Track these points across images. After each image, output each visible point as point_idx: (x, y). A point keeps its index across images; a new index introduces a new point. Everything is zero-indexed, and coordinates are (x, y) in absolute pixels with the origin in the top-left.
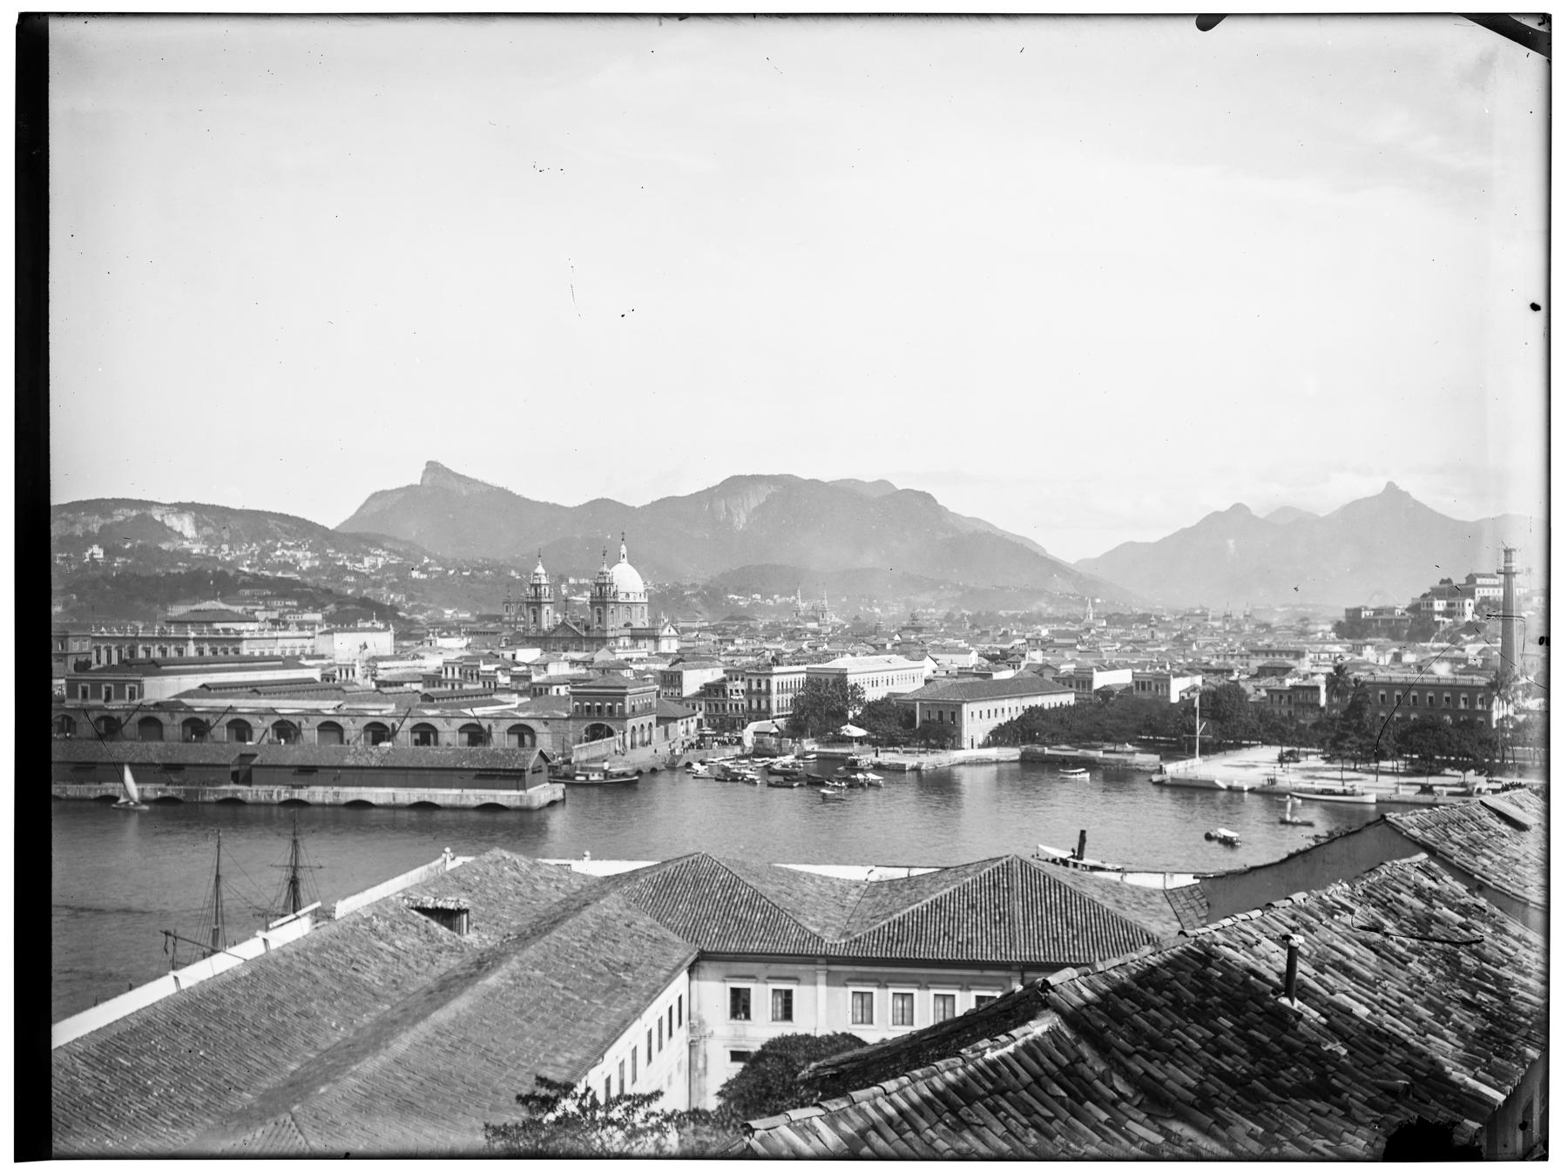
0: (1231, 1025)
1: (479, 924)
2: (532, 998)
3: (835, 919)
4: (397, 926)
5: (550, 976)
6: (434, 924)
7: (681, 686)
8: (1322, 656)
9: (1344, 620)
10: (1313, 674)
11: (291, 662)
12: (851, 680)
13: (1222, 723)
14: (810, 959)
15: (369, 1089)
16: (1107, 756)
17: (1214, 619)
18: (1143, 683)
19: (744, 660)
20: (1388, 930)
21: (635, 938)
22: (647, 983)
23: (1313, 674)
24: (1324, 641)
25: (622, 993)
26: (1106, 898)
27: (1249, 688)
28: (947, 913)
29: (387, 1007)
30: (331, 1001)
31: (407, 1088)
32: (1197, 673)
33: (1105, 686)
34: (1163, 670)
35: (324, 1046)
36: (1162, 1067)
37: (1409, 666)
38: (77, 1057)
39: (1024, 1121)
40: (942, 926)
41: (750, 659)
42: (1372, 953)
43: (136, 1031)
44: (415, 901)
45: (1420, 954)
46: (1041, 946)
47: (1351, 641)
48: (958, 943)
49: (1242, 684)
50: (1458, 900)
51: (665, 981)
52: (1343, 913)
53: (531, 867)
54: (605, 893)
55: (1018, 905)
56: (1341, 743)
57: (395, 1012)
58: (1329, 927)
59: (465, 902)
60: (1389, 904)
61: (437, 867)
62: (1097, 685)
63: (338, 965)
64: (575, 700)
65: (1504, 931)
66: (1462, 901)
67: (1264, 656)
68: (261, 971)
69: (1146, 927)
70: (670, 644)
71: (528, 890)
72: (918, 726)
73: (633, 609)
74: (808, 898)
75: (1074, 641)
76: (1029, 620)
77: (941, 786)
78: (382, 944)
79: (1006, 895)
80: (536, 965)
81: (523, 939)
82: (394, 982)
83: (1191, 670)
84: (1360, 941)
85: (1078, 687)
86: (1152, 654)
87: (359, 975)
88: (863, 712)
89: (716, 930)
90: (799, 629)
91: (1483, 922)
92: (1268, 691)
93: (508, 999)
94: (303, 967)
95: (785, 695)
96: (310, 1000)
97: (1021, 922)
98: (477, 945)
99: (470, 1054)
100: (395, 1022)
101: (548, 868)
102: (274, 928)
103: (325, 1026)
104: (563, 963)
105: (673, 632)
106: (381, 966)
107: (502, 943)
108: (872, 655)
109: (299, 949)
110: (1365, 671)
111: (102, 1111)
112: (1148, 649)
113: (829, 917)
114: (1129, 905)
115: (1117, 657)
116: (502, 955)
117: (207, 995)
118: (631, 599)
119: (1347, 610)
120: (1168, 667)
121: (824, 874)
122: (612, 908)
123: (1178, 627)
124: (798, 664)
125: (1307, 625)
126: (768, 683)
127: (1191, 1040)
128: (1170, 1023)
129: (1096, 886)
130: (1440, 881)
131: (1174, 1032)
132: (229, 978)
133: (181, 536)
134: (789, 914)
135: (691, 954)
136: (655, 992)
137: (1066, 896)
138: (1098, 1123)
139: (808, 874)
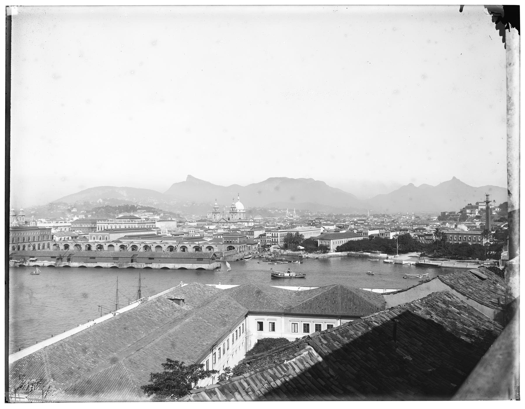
2: (198, 325)
5: (204, 319)
6: (174, 303)
8: (434, 226)
10: (431, 231)
16: (372, 254)
17: (403, 216)
18: (382, 234)
19: (271, 228)
21: (230, 307)
24: (435, 221)
26: (365, 296)
27: (412, 235)
29: (158, 327)
32: (398, 231)
38: (67, 343)
43: (85, 335)
44: (169, 297)
49: (411, 234)
52: (417, 310)
53: (204, 287)
55: (339, 298)
61: (179, 287)
64: (224, 239)
65: (473, 315)
67: (417, 225)
71: (202, 293)
75: (363, 222)
76: (352, 216)
78: (159, 309)
80: (200, 316)
81: (199, 307)
83: (396, 230)
86: (385, 226)
87: (151, 318)
91: (465, 311)
93: (191, 326)
94: (135, 316)
96: (136, 326)
98: (186, 309)
99: (178, 342)
104: (208, 315)
105: (252, 220)
107: (193, 309)
110: (446, 230)
113: (286, 302)
116: (192, 312)
117: (106, 324)
119: (441, 213)
123: (393, 218)
125: (430, 217)
130: (452, 298)
134: (274, 301)
135: (246, 312)
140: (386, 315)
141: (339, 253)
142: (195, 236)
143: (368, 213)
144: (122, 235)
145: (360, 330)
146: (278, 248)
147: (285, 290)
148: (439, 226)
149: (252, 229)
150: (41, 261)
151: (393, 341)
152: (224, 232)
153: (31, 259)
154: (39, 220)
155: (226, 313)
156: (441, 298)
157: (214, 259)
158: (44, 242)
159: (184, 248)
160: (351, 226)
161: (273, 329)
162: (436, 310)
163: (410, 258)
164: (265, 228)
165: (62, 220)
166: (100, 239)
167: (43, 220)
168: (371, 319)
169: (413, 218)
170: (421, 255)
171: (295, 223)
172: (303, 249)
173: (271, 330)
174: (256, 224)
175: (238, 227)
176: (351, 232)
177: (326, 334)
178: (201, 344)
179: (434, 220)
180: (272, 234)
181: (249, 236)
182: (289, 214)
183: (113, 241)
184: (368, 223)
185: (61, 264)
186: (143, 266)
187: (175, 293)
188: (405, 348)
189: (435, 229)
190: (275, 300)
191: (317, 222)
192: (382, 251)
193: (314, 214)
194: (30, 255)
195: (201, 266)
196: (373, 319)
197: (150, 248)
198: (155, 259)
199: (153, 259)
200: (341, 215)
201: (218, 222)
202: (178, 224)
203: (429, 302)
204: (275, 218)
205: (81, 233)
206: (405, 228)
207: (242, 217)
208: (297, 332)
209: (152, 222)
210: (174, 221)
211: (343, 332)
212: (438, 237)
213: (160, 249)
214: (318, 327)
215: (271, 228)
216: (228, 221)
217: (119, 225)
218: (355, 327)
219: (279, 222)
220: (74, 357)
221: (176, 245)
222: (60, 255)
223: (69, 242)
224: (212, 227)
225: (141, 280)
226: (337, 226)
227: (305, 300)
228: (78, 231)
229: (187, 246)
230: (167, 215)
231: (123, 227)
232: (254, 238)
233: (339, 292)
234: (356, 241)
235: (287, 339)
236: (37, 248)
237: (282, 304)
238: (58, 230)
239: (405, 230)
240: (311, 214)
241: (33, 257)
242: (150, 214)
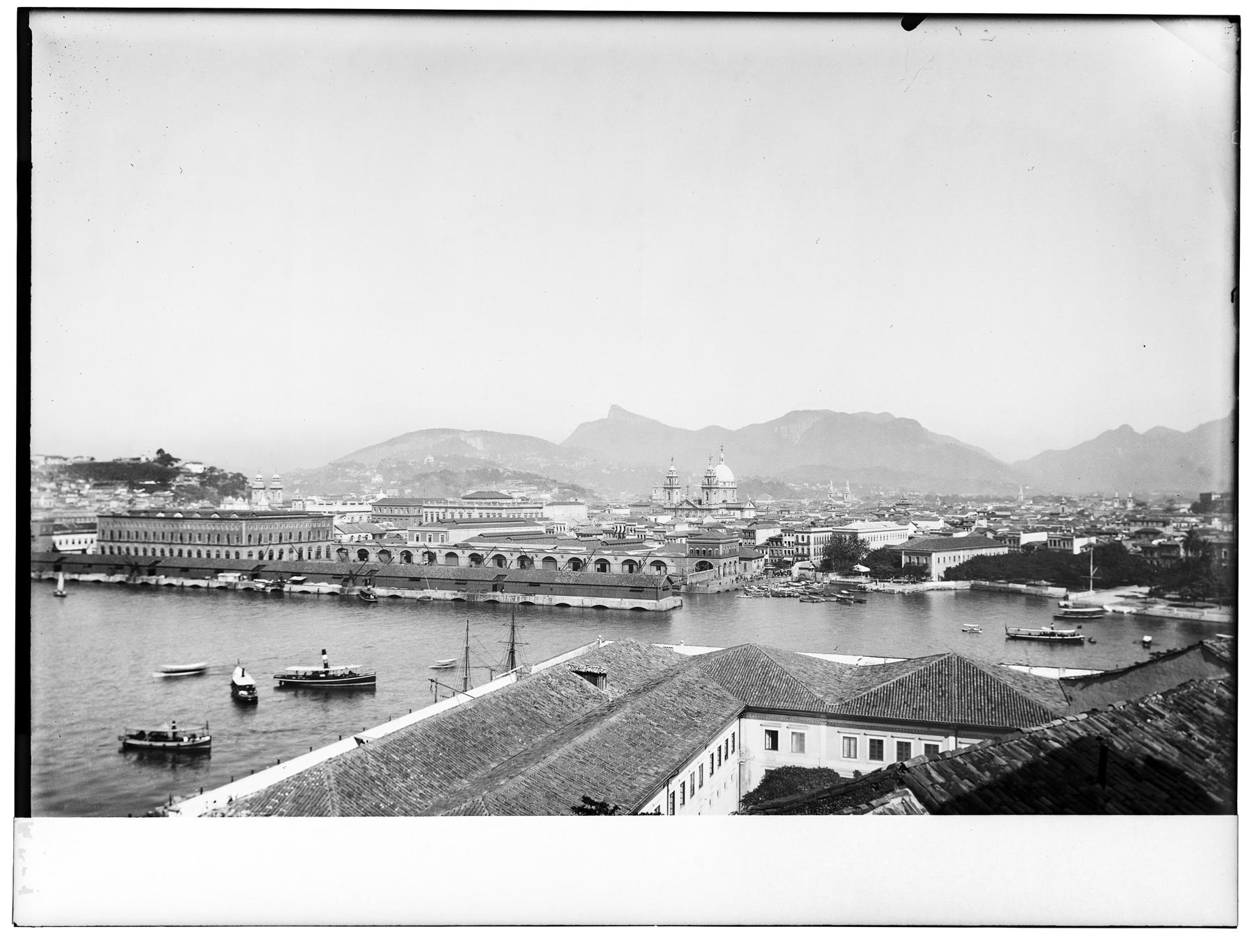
0: (1050, 803)
3: (834, 689)
6: (585, 682)
7: (755, 539)
8: (1183, 525)
9: (1199, 501)
10: (1175, 537)
11: (526, 522)
12: (861, 537)
15: (531, 784)
16: (1030, 588)
17: (1107, 500)
19: (795, 523)
20: (1191, 732)
21: (706, 696)
22: (710, 725)
23: (1175, 537)
26: (1016, 684)
27: (1129, 545)
28: (907, 689)
30: (518, 725)
31: (554, 784)
32: (1092, 536)
33: (1028, 543)
34: (1069, 533)
35: (513, 754)
40: (903, 697)
41: (799, 523)
42: (1176, 750)
43: (405, 739)
45: (1217, 751)
46: (970, 714)
47: (1204, 515)
48: (913, 709)
49: (1124, 543)
51: (721, 724)
52: (1155, 718)
56: (1194, 583)
57: (557, 735)
58: (1142, 728)
59: (604, 669)
60: (1195, 712)
61: (594, 646)
63: (526, 704)
67: (1140, 523)
68: (481, 705)
69: (1043, 705)
70: (750, 513)
72: (903, 566)
74: (817, 675)
75: (1009, 513)
76: (981, 500)
77: (918, 601)
78: (553, 693)
79: (947, 679)
80: (641, 710)
81: (637, 693)
82: (559, 716)
83: (1088, 533)
84: (1167, 740)
85: (1010, 542)
86: (1061, 523)
87: (538, 711)
88: (869, 556)
89: (757, 693)
90: (831, 505)
92: (1142, 548)
93: (622, 731)
94: (505, 705)
95: (819, 545)
96: (508, 725)
97: (956, 697)
100: (555, 741)
105: (752, 506)
106: (552, 706)
107: (625, 696)
108: (875, 521)
110: (1213, 535)
111: (380, 786)
112: (1060, 519)
113: (830, 688)
115: (1038, 524)
116: (623, 703)
117: (447, 720)
118: (727, 486)
120: (1073, 531)
121: (829, 660)
123: (1081, 505)
124: (827, 526)
125: (1172, 504)
126: (808, 537)
129: (1009, 675)
131: (1002, 807)
132: (460, 709)
134: (804, 685)
136: (715, 733)
137: (987, 681)
140: (1081, 726)
141: (952, 584)
143: (1021, 492)
144: (475, 533)
145: (1020, 757)
146: (810, 569)
147: (829, 663)
149: (751, 525)
150: (312, 584)
151: (1098, 786)
153: (295, 578)
154: (309, 498)
156: (1212, 692)
157: (668, 589)
158: (320, 544)
159: (603, 565)
160: (981, 522)
161: (802, 749)
162: (1201, 719)
163: (1122, 599)
164: (781, 522)
165: (353, 499)
166: (430, 540)
167: (317, 499)
168: (1045, 733)
169: (1130, 506)
170: (1151, 594)
171: (848, 514)
172: (866, 572)
173: (794, 750)
174: (759, 513)
175: (720, 521)
176: (978, 535)
177: (942, 762)
178: (643, 771)
179: (1182, 511)
181: (745, 541)
182: (836, 494)
183: (456, 546)
185: (353, 591)
186: (516, 600)
187: (587, 660)
188: (1128, 803)
189: (1184, 534)
191: (899, 513)
192: (1050, 581)
193: (893, 494)
194: (293, 570)
195: (640, 603)
196: (1048, 732)
197: (532, 561)
198: (541, 585)
199: (537, 584)
200: (956, 499)
201: (675, 509)
202: (591, 511)
203: (1184, 701)
204: (803, 501)
205: (391, 526)
206: (1113, 529)
207: (731, 498)
208: (856, 757)
210: (582, 504)
211: (979, 758)
212: (1191, 552)
213: (551, 565)
214: (904, 749)
215: (795, 523)
216: (698, 506)
217: (467, 511)
218: (1009, 749)
219: (812, 511)
221: (585, 557)
222: (351, 571)
223: (367, 544)
224: (663, 519)
225: (516, 629)
226: (947, 522)
227: (874, 686)
228: (385, 523)
229: (610, 559)
231: (475, 514)
232: (757, 545)
233: (955, 671)
234: (991, 557)
235: (835, 771)
236: (305, 556)
238: (347, 520)
239: (1110, 534)
240: (885, 494)
241: (299, 574)
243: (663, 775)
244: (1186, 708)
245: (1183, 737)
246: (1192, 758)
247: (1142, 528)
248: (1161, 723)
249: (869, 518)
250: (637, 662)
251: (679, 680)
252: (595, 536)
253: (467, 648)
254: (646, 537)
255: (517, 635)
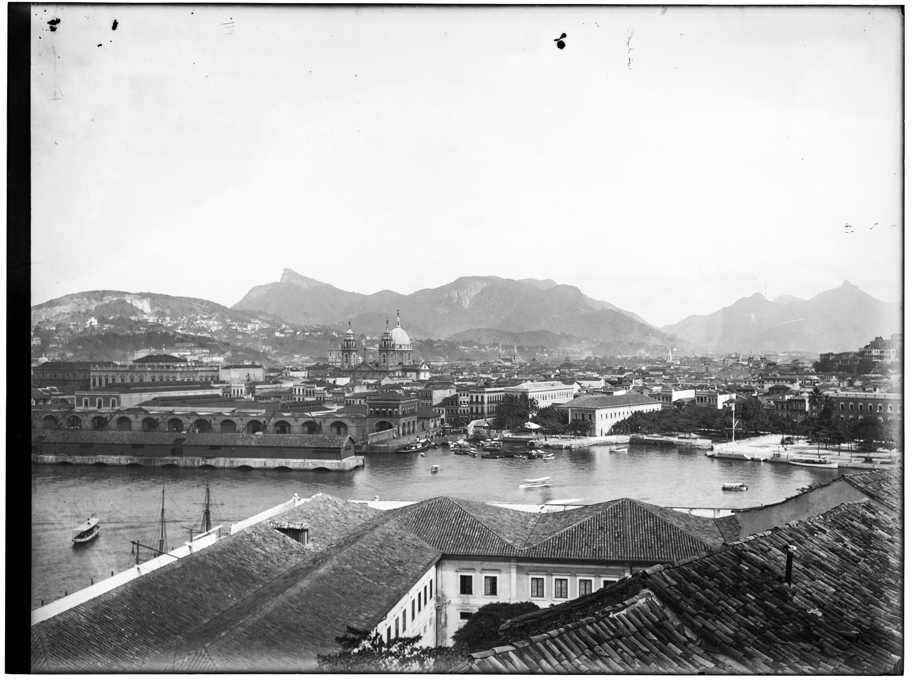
0: (754, 598)
1: (314, 538)
3: (522, 535)
4: (267, 539)
5: (355, 568)
6: (289, 538)
8: (807, 382)
10: (802, 393)
12: (530, 396)
13: (748, 421)
14: (507, 559)
16: (681, 440)
18: (702, 398)
19: (469, 383)
21: (405, 546)
23: (802, 393)
25: (397, 578)
26: (680, 524)
27: (764, 401)
28: (587, 532)
29: (261, 586)
30: (228, 583)
31: (272, 633)
32: (733, 392)
33: (679, 400)
34: (713, 391)
35: (224, 609)
36: (713, 623)
37: (858, 388)
38: (82, 615)
39: (633, 654)
40: (584, 539)
41: (472, 383)
42: (836, 556)
44: (277, 524)
45: (865, 557)
48: (593, 549)
49: (759, 398)
50: (887, 525)
51: (422, 571)
52: (820, 533)
54: (387, 520)
57: (265, 589)
59: (306, 525)
62: (674, 399)
63: (232, 561)
64: (370, 408)
66: (890, 526)
67: (773, 382)
69: (704, 541)
70: (425, 374)
72: (570, 423)
73: (404, 355)
74: (506, 523)
78: (258, 549)
79: (622, 521)
80: (347, 562)
82: (265, 571)
83: (730, 390)
84: (830, 549)
85: (663, 400)
87: (245, 568)
89: (452, 542)
90: (500, 366)
94: (212, 562)
96: (216, 582)
97: (630, 537)
98: (313, 550)
100: (265, 595)
101: (354, 505)
102: (195, 540)
103: (224, 597)
104: (363, 561)
105: (427, 368)
107: (327, 549)
108: (543, 381)
109: (209, 553)
110: (832, 390)
111: (96, 646)
112: (704, 378)
113: (518, 535)
114: (694, 528)
115: (686, 382)
118: (403, 348)
120: (716, 389)
121: (515, 509)
122: (391, 529)
124: (500, 387)
125: (798, 364)
126: (482, 397)
127: (730, 607)
128: (718, 597)
129: (674, 516)
130: (877, 514)
133: (142, 312)
134: (494, 532)
135: (437, 556)
136: (416, 578)
137: (656, 522)
138: (676, 656)
139: (506, 509)
142: (307, 399)
147: (515, 512)
148: (817, 382)
152: (368, 391)
155: (397, 558)
160: (637, 381)
162: (851, 533)
164: (456, 383)
174: (434, 375)
178: (354, 618)
180: (472, 397)
184: (671, 374)
190: (497, 531)
202: (268, 374)
204: (473, 363)
209: (212, 369)
215: (469, 383)
216: (375, 369)
220: (100, 643)
225: (211, 495)
227: (558, 531)
230: (241, 355)
237: (511, 539)
242: (203, 353)
243: (373, 619)
244: (840, 525)
245: (841, 546)
246: (848, 561)
247: (773, 385)
248: (824, 537)
249: (537, 379)
250: (335, 518)
251: (379, 532)
252: (273, 399)
253: (163, 510)
254: (326, 399)
255: (212, 497)
